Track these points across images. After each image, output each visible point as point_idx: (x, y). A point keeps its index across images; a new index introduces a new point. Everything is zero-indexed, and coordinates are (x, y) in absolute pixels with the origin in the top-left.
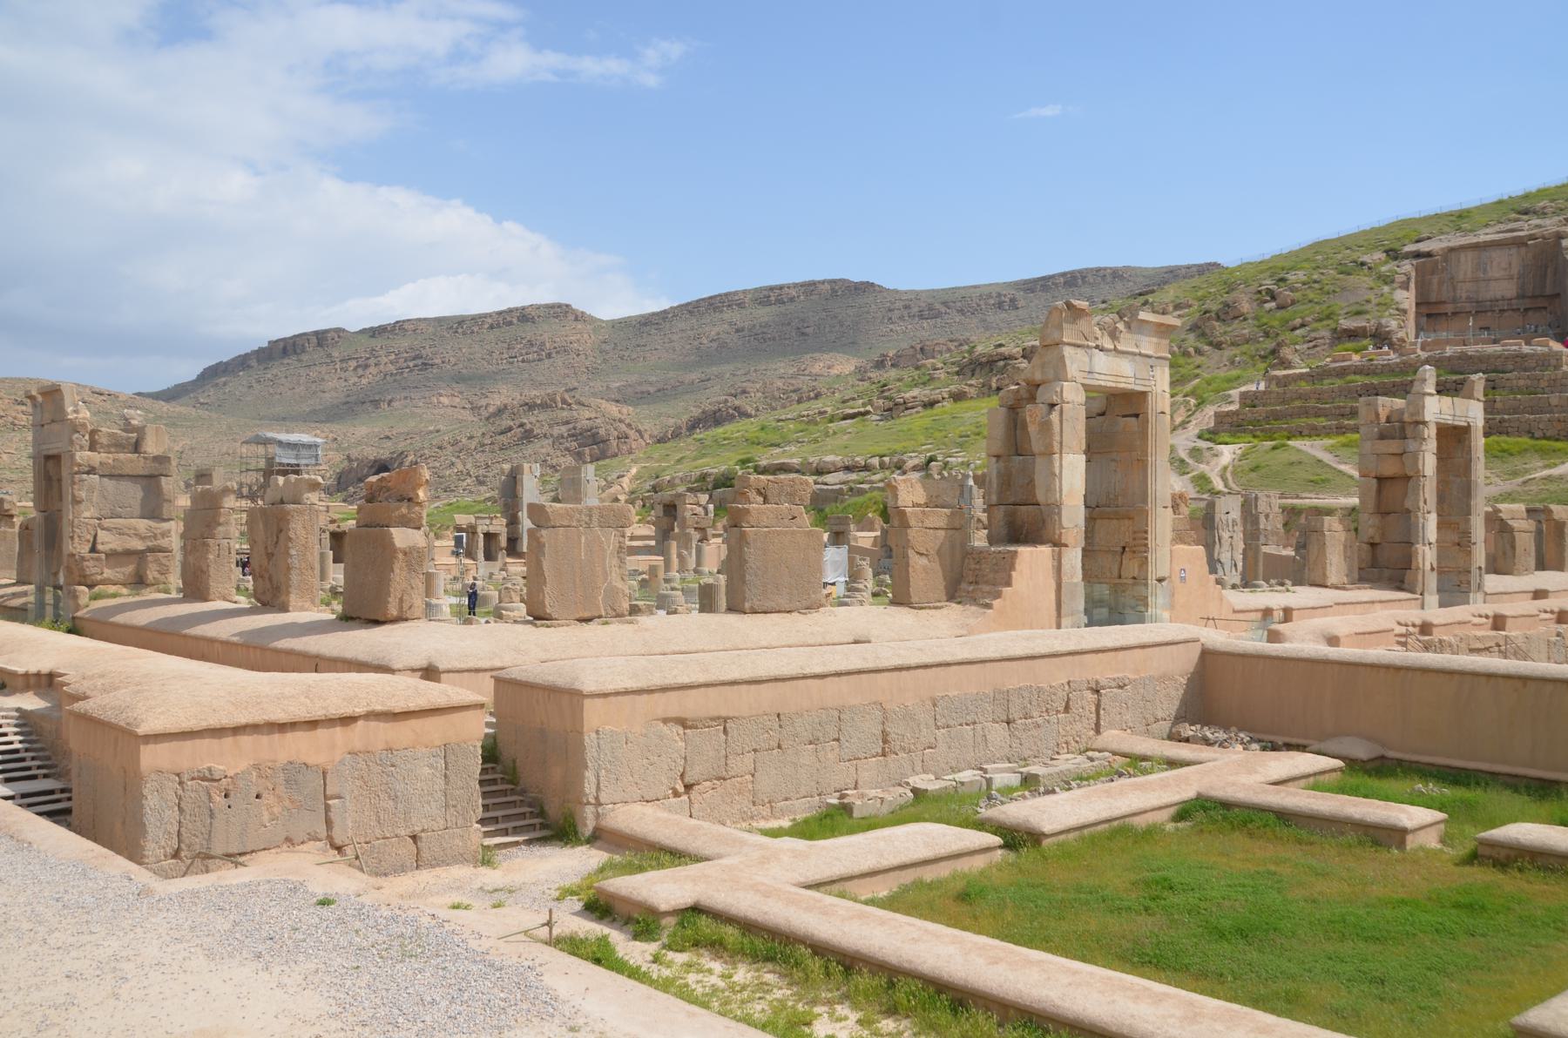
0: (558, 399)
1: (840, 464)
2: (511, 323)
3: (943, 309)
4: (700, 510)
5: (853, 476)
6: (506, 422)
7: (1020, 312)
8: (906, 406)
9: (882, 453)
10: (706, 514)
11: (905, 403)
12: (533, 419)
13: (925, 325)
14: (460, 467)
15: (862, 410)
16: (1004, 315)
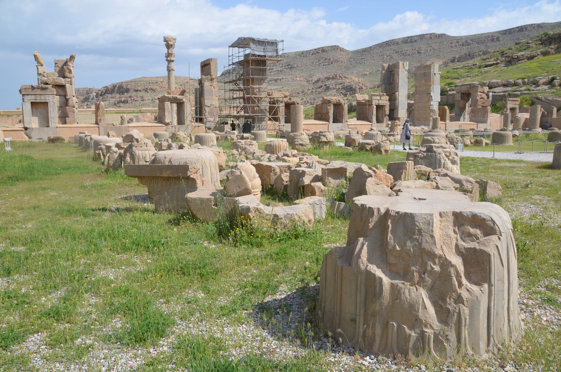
0: (338, 76)
1: (500, 84)
2: (319, 53)
3: (471, 42)
4: (484, 96)
5: (509, 89)
6: (320, 84)
7: (501, 42)
8: (518, 59)
9: (524, 77)
10: (488, 98)
11: (518, 58)
12: (329, 83)
13: (464, 48)
14: (305, 99)
15: (495, 62)
16: (494, 43)
